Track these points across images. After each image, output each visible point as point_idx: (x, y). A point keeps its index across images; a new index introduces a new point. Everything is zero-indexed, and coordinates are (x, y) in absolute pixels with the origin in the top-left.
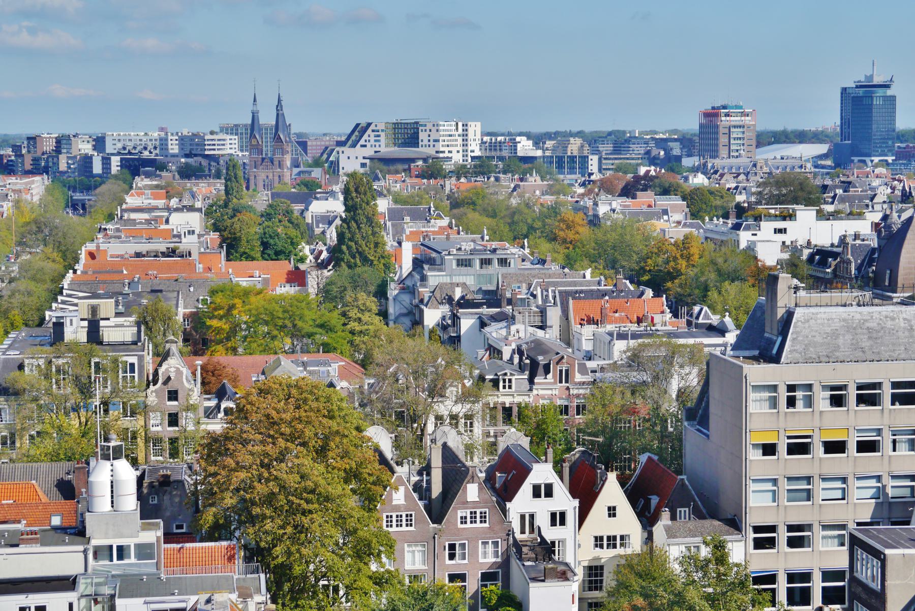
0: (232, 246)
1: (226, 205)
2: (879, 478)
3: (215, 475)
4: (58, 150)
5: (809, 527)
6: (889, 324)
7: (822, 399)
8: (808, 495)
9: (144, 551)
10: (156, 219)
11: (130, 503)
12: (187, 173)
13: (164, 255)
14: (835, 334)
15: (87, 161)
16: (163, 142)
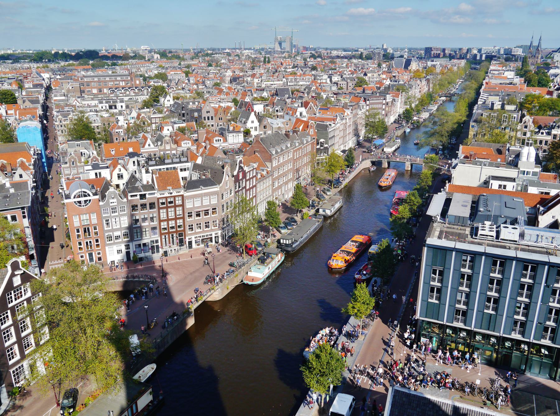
0: (529, 82)
1: (521, 69)
3: (555, 154)
4: (467, 52)
9: (535, 174)
10: (501, 73)
11: (533, 159)
12: (507, 60)
13: (508, 84)
15: (475, 56)
16: (499, 50)
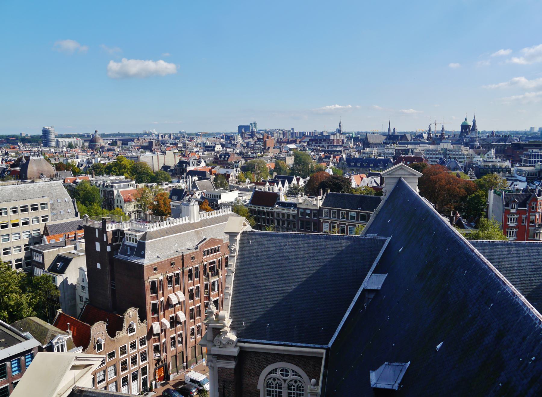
2: (29, 232)
5: (10, 248)
6: (27, 189)
7: (10, 212)
8: (9, 239)
14: (11, 193)
